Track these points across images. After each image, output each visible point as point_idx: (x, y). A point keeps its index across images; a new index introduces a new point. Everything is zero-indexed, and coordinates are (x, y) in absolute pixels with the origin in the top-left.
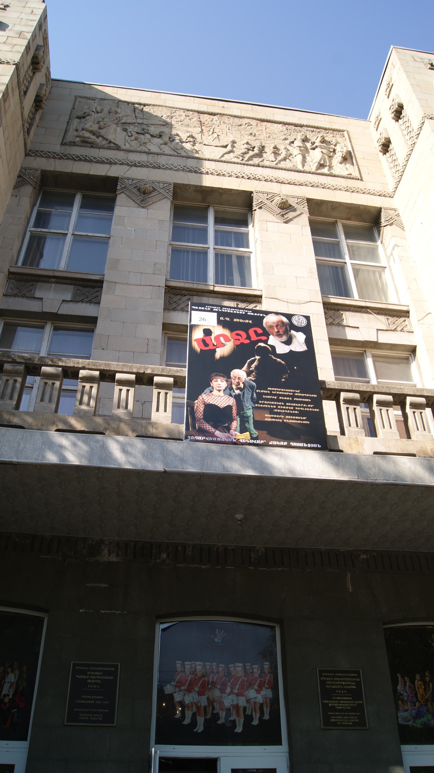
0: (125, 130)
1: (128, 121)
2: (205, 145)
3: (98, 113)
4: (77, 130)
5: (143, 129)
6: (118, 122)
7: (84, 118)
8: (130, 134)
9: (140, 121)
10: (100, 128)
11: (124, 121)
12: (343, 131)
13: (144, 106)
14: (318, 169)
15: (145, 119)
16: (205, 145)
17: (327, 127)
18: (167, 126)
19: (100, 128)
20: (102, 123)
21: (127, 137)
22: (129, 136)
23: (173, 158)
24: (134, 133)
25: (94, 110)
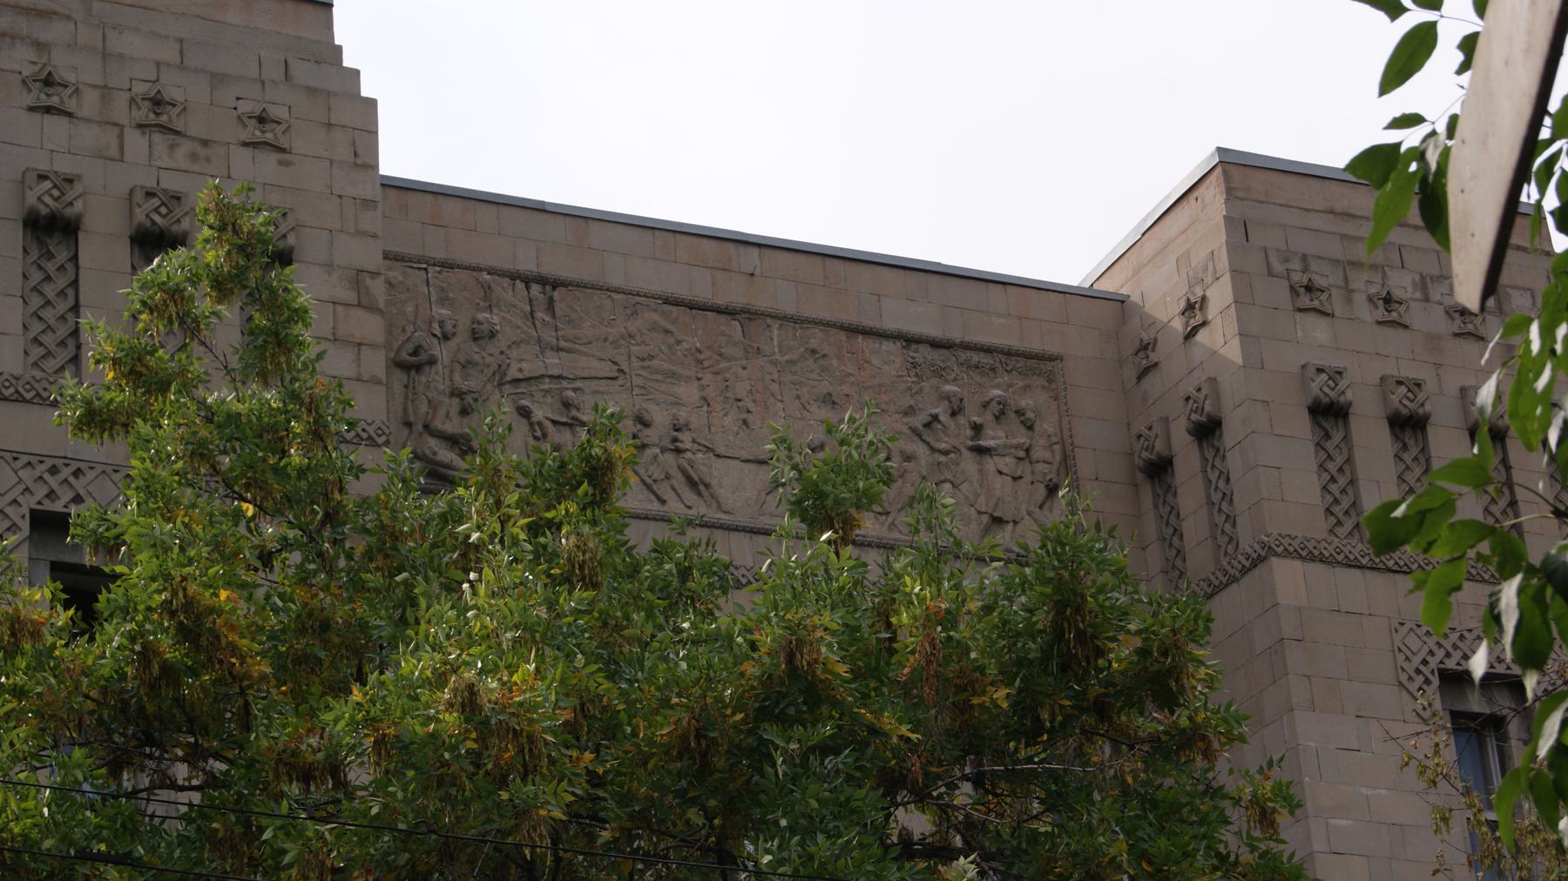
0: (524, 413)
1: (529, 368)
2: (718, 456)
3: (446, 337)
4: (408, 425)
5: (567, 405)
6: (500, 379)
7: (418, 368)
8: (539, 434)
9: (553, 363)
10: (464, 412)
11: (513, 373)
12: (1052, 358)
13: (554, 288)
14: (986, 531)
15: (559, 349)
16: (718, 456)
17: (1014, 343)
18: (620, 382)
19: (464, 412)
20: (469, 399)
21: (532, 442)
22: (536, 438)
23: (652, 524)
24: (550, 427)
25: (438, 332)
